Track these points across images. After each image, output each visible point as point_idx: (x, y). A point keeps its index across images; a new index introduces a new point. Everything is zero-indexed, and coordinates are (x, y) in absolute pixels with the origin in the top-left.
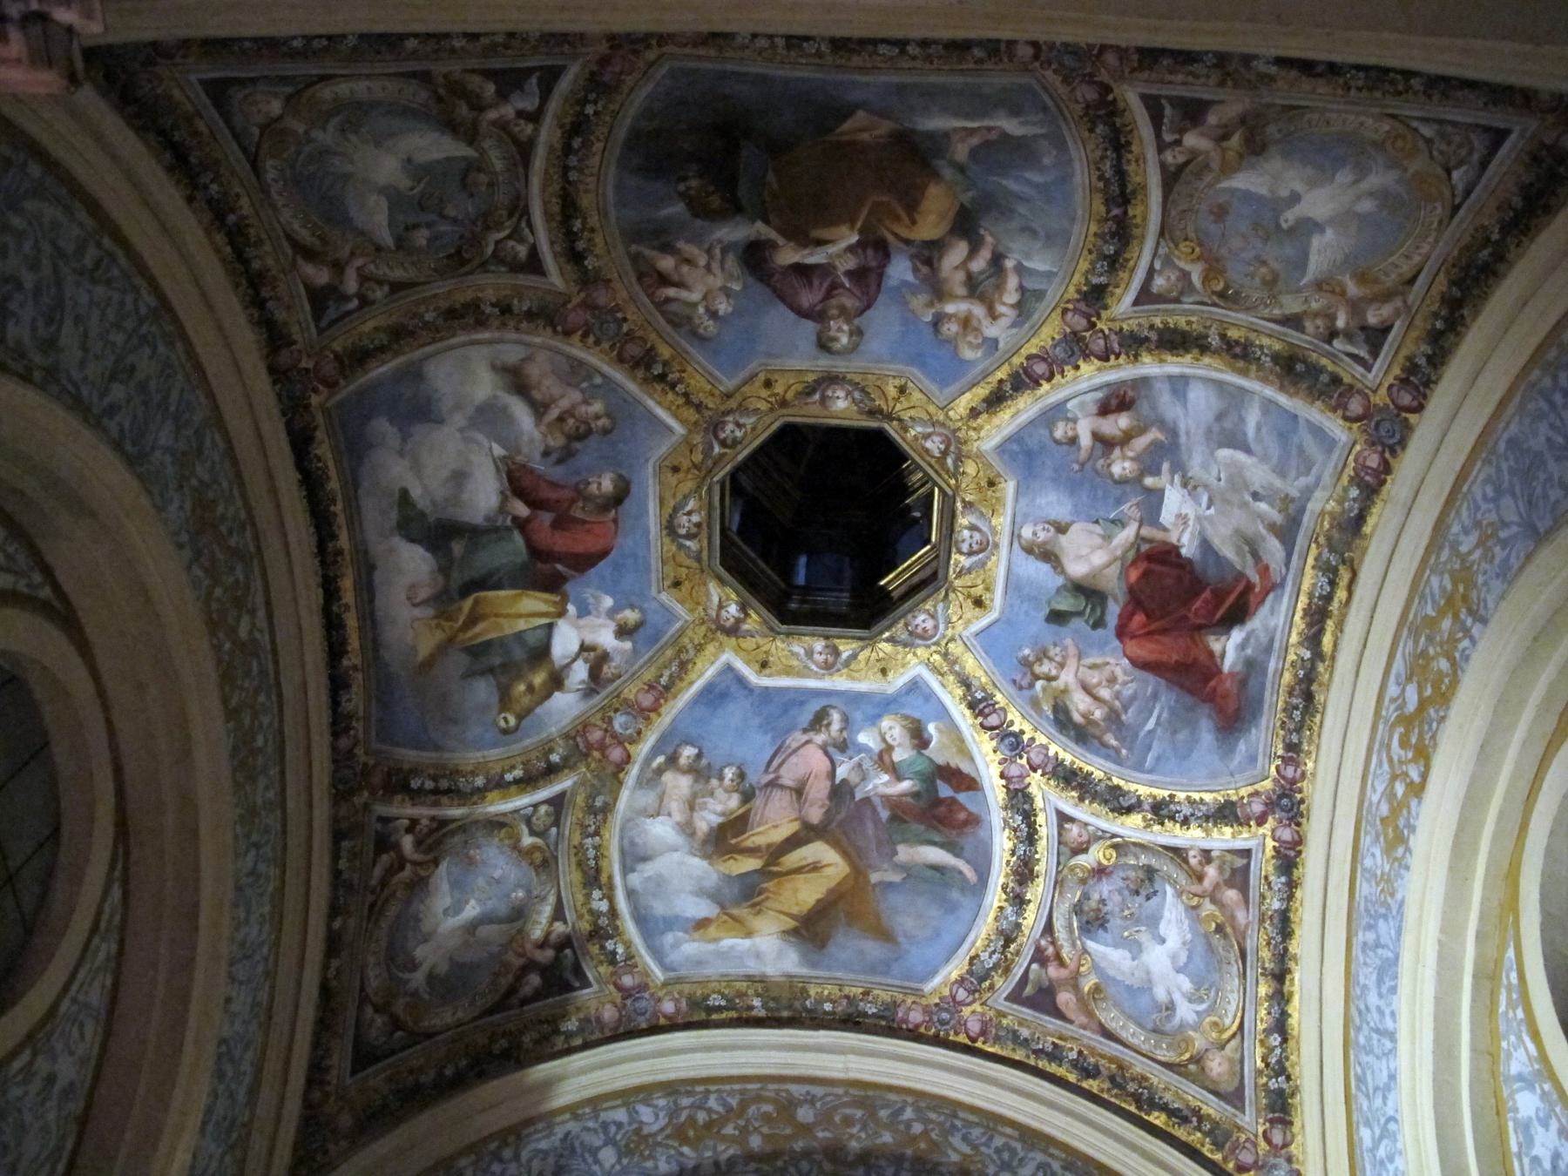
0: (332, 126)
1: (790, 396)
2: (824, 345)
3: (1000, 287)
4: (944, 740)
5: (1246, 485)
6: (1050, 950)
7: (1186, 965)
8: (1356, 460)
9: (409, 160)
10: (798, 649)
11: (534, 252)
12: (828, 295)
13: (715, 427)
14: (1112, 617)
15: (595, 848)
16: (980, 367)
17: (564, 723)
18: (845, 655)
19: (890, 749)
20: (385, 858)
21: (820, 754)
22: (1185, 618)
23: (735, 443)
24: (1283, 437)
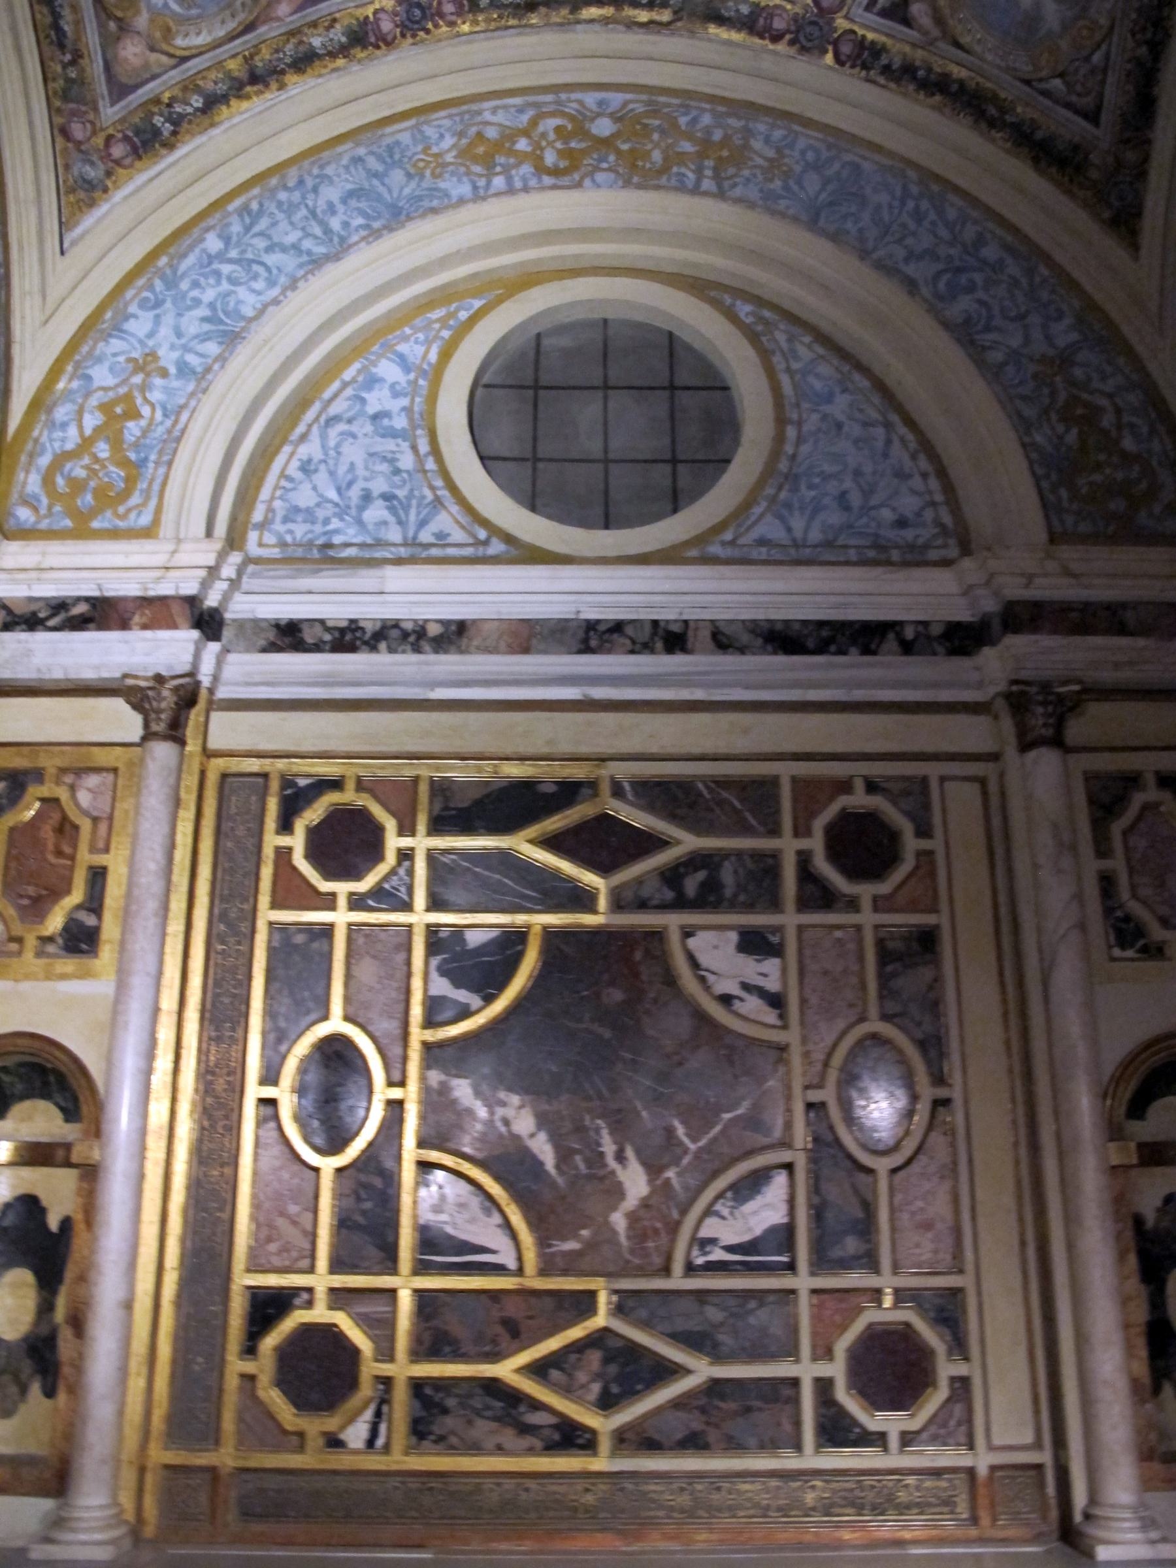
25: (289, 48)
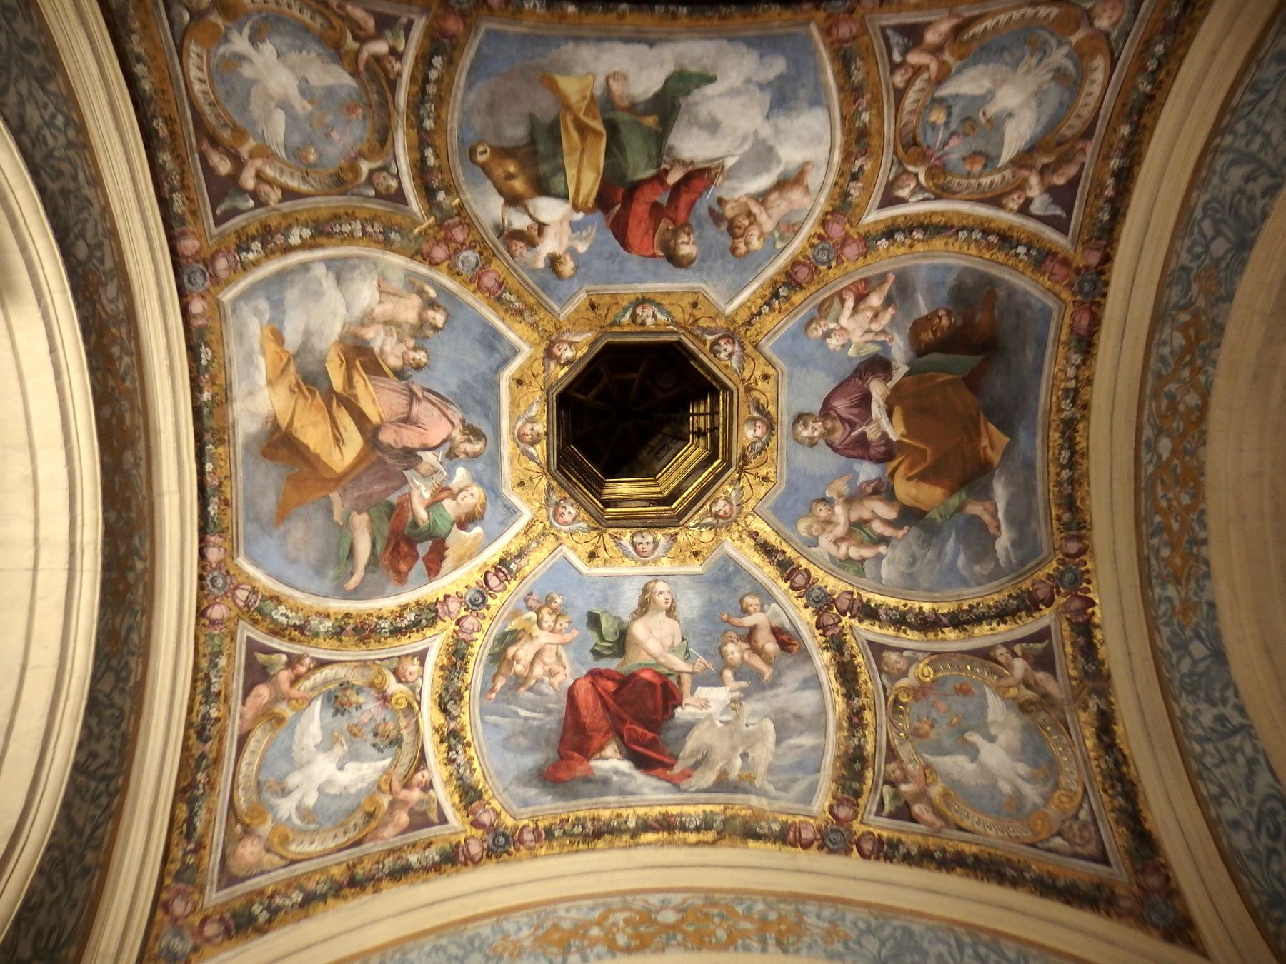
0: (1069, 65)
1: (755, 394)
2: (800, 418)
3: (861, 544)
4: (468, 543)
5: (751, 746)
6: (302, 669)
7: (327, 795)
8: (801, 822)
9: (1010, 115)
10: (535, 410)
11: (902, 201)
12: (843, 420)
13: (730, 337)
14: (603, 664)
15: (351, 232)
16: (794, 537)
17: (472, 204)
18: (531, 450)
19: (454, 496)
20: (370, 23)
21: (444, 436)
22: (623, 721)
23: (715, 353)
24: (800, 766)
25: (389, 862)
